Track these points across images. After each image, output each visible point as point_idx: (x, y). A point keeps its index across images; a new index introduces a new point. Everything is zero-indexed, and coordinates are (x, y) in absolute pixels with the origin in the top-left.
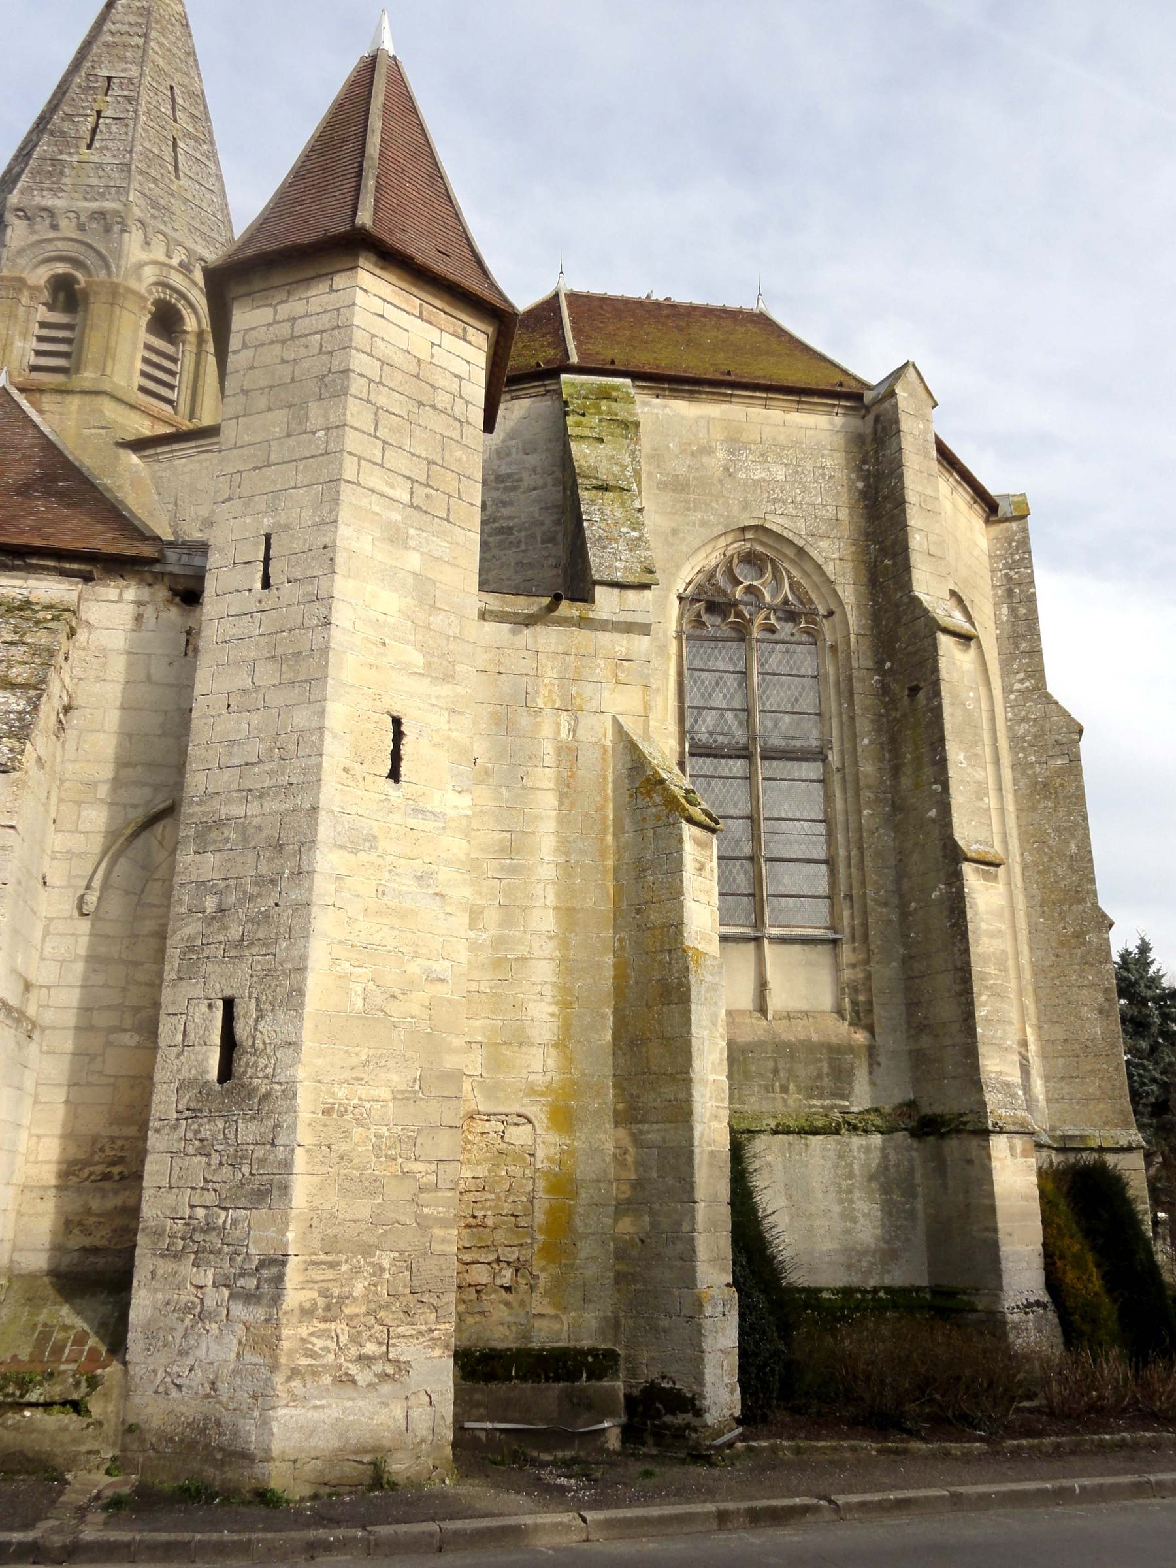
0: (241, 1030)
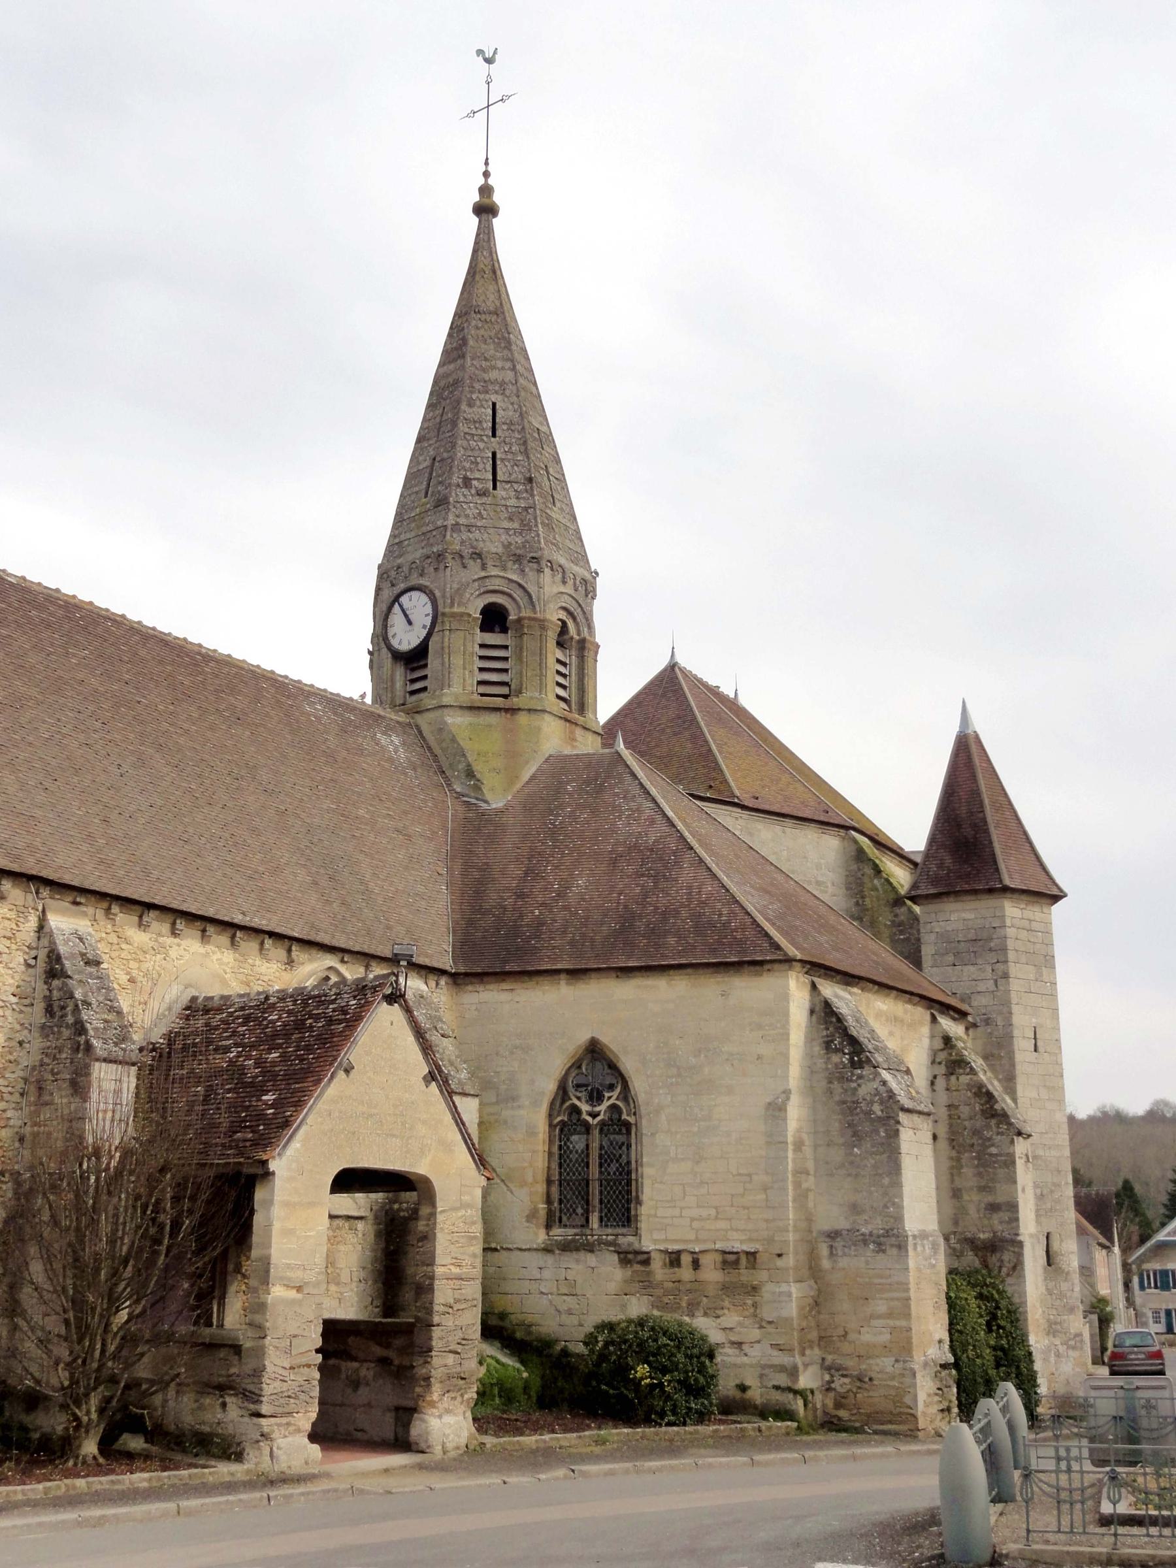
0: (1055, 1246)
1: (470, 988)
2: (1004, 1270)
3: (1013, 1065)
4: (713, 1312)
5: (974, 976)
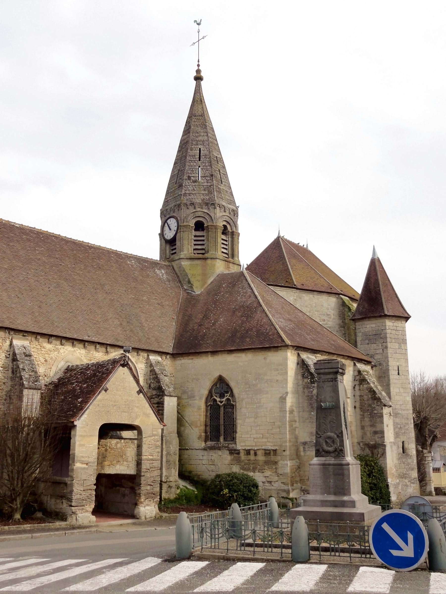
0: (406, 446)
1: (178, 359)
2: (379, 455)
3: (389, 380)
4: (261, 471)
5: (375, 348)
